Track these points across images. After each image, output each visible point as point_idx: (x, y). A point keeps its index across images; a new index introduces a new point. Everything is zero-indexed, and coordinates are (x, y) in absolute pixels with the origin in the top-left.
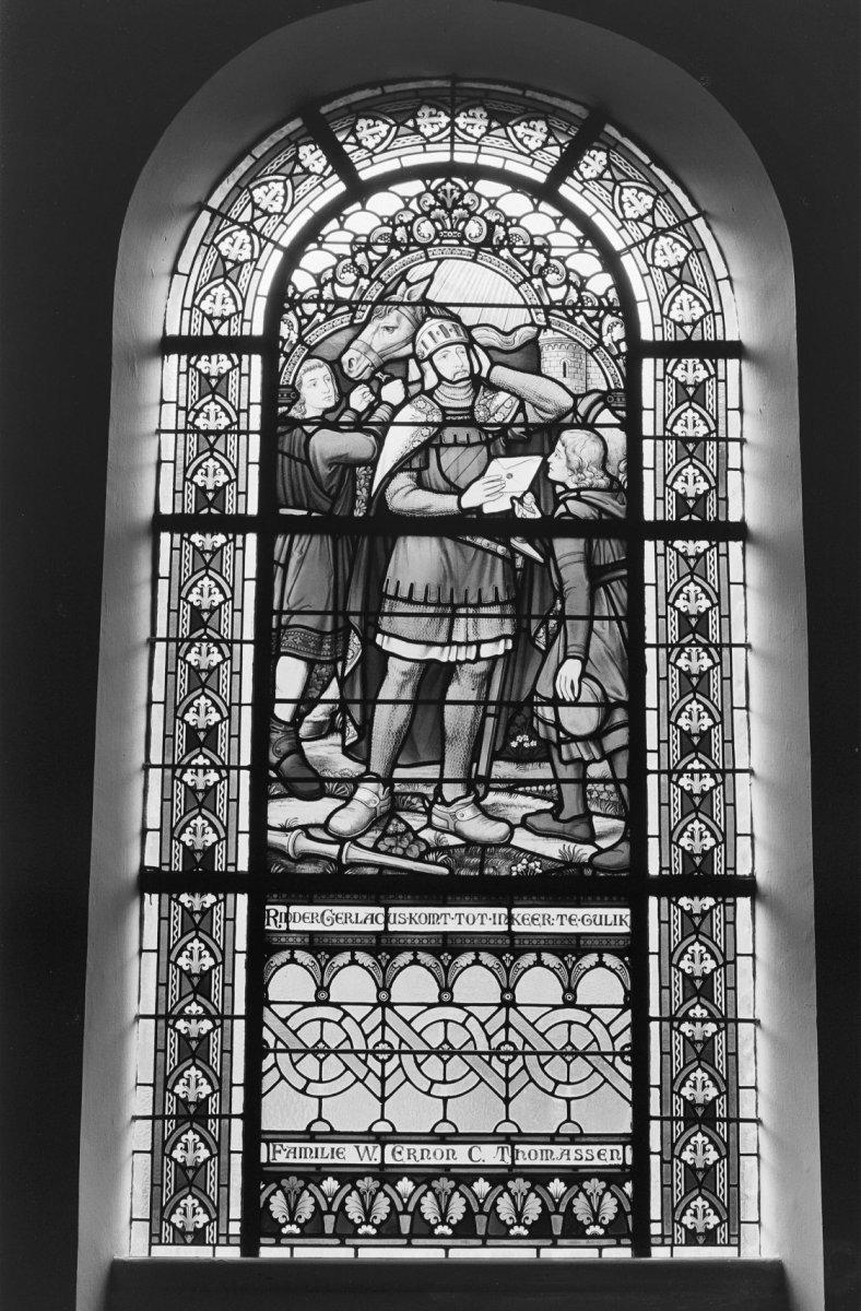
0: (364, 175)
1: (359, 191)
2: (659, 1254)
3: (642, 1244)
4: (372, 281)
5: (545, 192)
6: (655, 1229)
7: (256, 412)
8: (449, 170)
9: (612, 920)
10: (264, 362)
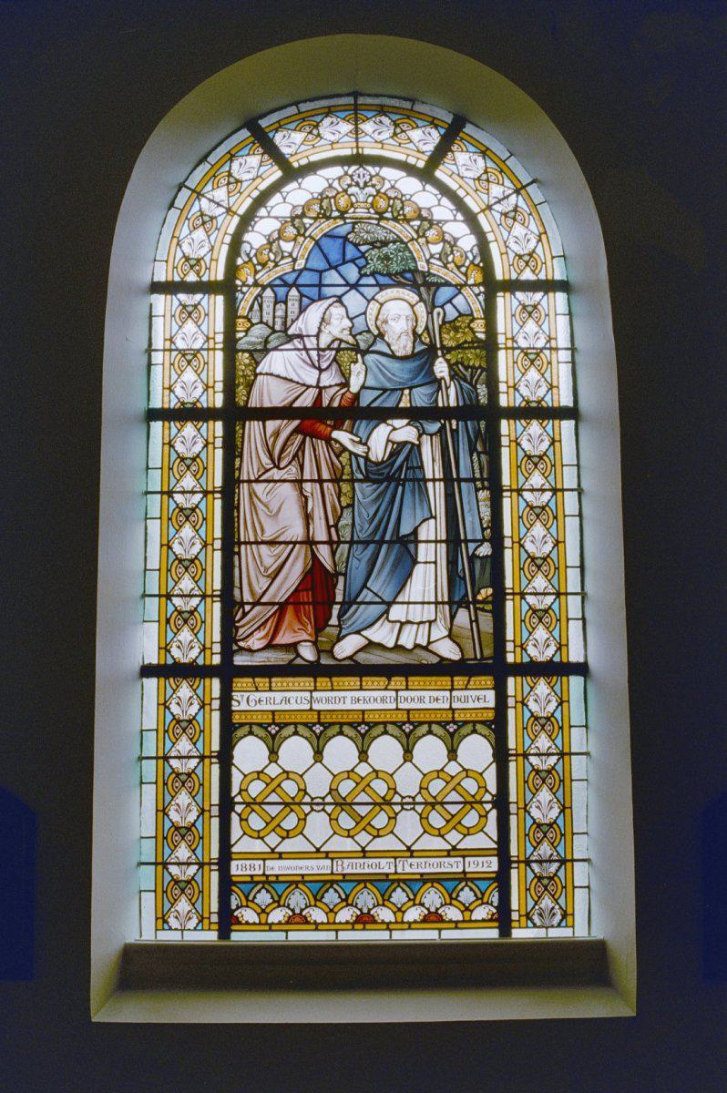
2: (519, 934)
3: (505, 928)
4: (306, 238)
5: (426, 174)
6: (515, 916)
7: (217, 648)
8: (359, 159)
9: (479, 697)
10: (222, 683)
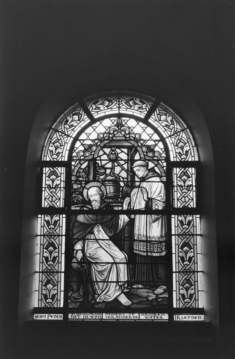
0: (95, 117)
1: (93, 121)
4: (97, 147)
5: (145, 121)
8: (119, 116)
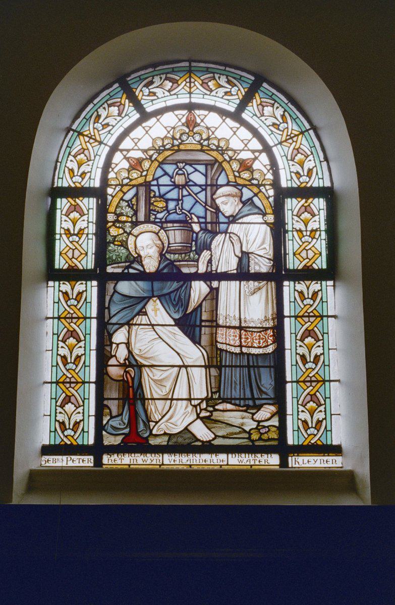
1: (145, 116)
4: (152, 162)
5: (236, 116)
8: (191, 107)
